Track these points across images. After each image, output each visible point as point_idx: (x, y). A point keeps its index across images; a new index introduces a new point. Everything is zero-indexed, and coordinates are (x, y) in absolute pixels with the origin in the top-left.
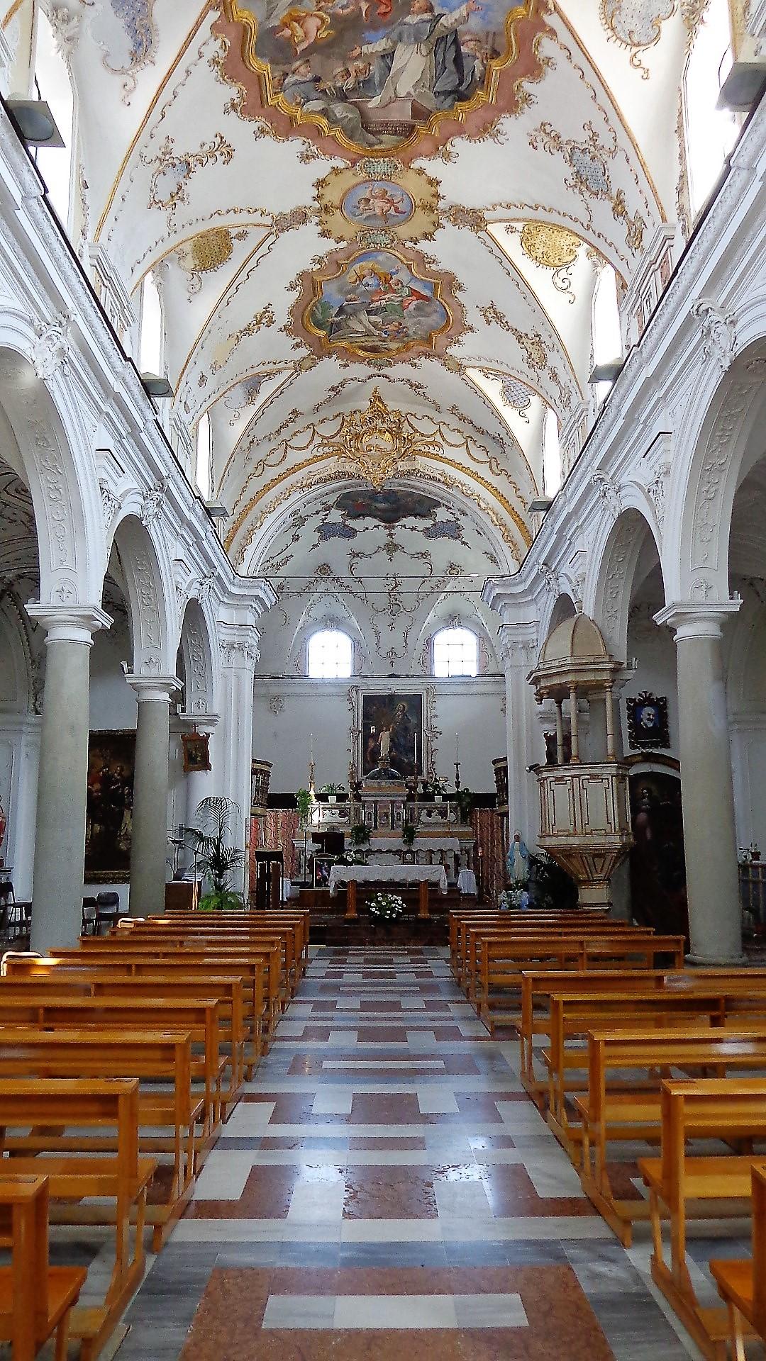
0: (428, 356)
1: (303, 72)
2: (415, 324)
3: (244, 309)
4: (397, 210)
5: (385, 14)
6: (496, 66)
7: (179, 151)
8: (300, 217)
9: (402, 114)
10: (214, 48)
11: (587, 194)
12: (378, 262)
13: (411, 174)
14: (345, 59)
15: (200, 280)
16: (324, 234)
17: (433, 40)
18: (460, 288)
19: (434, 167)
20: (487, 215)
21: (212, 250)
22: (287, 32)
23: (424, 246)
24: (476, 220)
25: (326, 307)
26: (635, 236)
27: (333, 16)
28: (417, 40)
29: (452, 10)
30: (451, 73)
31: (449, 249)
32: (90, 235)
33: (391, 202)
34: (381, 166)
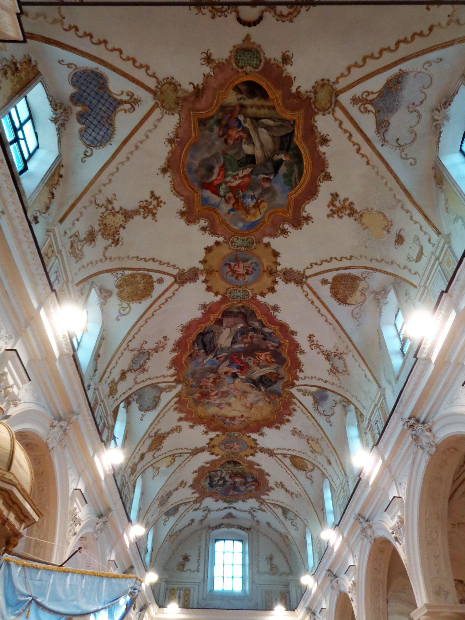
1: (270, 344)
2: (213, 144)
4: (230, 266)
9: (227, 321)
12: (243, 220)
14: (251, 343)
17: (216, 350)
18: (182, 214)
19: (211, 298)
20: (176, 286)
27: (255, 358)
33: (233, 271)
34: (239, 294)
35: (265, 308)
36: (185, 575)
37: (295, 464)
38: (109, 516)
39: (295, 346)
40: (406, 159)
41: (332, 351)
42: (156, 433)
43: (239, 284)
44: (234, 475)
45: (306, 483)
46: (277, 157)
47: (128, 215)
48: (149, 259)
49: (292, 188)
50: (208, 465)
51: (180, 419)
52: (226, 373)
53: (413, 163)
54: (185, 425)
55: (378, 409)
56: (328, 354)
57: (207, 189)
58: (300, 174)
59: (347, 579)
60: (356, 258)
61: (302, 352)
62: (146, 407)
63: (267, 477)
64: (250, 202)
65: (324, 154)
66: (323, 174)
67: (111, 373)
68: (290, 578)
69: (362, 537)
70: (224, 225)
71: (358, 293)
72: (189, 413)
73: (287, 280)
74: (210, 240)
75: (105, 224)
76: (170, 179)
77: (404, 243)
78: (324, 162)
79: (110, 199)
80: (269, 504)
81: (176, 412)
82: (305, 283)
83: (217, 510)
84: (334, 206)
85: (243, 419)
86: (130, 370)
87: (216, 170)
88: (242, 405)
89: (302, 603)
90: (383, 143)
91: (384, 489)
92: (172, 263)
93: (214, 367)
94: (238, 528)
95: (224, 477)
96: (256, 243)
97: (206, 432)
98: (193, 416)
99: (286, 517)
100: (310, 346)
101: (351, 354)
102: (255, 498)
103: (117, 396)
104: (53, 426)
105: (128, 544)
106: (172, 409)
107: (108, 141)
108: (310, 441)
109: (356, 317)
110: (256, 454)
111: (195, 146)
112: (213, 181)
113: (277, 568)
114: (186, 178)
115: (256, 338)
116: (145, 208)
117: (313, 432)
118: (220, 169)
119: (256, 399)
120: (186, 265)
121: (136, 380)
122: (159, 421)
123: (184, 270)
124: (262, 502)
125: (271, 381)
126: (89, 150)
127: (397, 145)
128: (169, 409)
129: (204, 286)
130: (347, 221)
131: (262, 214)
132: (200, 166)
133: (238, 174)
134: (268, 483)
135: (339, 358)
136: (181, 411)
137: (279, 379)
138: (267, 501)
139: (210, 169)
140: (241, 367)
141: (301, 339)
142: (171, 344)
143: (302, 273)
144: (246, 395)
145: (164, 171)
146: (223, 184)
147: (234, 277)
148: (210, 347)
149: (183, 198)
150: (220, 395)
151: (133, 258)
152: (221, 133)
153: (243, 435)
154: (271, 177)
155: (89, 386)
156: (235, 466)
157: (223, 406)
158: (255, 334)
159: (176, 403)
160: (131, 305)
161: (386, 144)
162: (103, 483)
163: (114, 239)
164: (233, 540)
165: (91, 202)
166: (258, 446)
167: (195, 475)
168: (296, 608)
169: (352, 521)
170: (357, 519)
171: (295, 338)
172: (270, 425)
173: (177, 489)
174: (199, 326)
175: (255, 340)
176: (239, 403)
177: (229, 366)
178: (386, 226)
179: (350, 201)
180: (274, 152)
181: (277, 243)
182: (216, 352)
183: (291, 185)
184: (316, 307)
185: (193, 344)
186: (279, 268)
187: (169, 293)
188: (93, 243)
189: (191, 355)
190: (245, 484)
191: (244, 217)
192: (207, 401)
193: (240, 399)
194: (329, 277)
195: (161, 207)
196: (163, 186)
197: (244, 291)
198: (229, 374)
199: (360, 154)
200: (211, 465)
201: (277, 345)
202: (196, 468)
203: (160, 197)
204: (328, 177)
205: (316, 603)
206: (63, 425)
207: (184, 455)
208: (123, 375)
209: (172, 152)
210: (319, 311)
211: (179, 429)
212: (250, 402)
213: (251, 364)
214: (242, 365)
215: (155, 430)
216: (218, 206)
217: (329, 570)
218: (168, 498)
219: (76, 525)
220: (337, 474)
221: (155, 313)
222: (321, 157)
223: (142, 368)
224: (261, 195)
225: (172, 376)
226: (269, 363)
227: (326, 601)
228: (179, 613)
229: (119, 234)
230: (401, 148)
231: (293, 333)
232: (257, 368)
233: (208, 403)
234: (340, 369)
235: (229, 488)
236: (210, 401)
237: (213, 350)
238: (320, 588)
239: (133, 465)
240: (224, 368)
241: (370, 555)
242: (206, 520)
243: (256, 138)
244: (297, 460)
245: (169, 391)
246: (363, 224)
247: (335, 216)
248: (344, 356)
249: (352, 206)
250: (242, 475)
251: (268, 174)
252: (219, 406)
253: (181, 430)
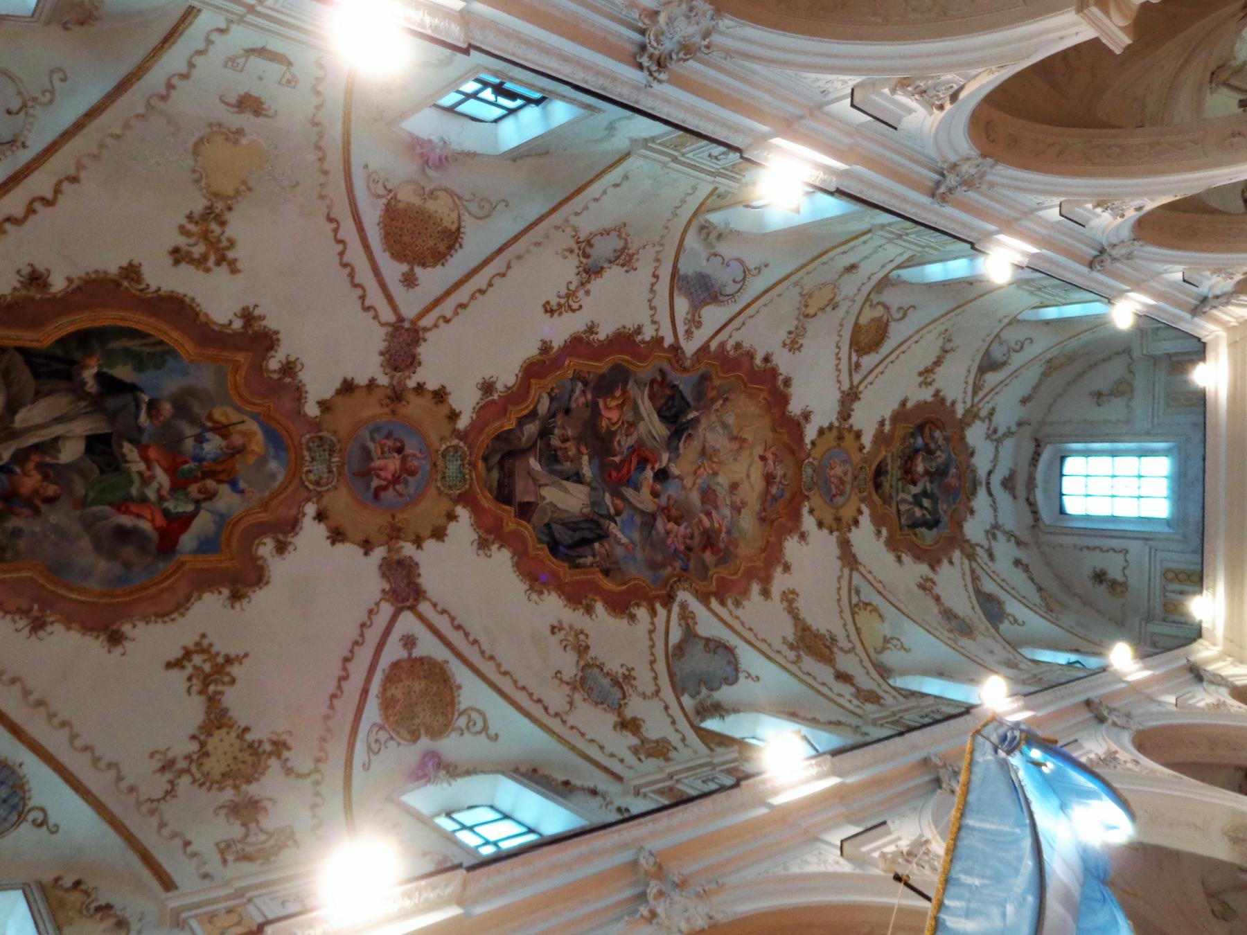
1: (579, 399)
2: (56, 529)
4: (379, 490)
5: (610, 476)
9: (523, 492)
12: (263, 460)
13: (445, 505)
14: (580, 439)
15: (379, 197)
17: (596, 517)
18: (236, 597)
19: (463, 528)
22: (618, 393)
27: (614, 434)
29: (622, 531)
34: (453, 468)
36: (1132, 581)
37: (875, 345)
38: (939, 763)
39: (577, 344)
40: (52, 92)
41: (577, 263)
42: (791, 647)
43: (428, 467)
44: (909, 476)
45: (915, 319)
46: (91, 386)
47: (217, 719)
48: (345, 669)
49: (172, 352)
50: (884, 531)
51: (766, 593)
52: (655, 494)
53: (61, 75)
54: (780, 582)
55: (683, 155)
56: (587, 271)
57: (175, 542)
58: (133, 333)
59: (1095, 222)
60: (329, 207)
61: (591, 329)
62: (729, 669)
63: (909, 405)
64: (213, 445)
65: (70, 280)
66: (126, 283)
67: (612, 755)
68: (1136, 354)
69: (984, 187)
70: (275, 502)
71: (431, 206)
72: (750, 574)
73: (412, 363)
74: (312, 533)
75: (223, 775)
76: (141, 625)
77: (255, 93)
78: (94, 280)
79: (160, 765)
80: (976, 400)
81: (745, 603)
82: (414, 322)
83: (995, 510)
84: (204, 258)
85: (769, 456)
86: (619, 709)
87: (126, 520)
88: (735, 459)
89: (1183, 326)
90: (19, 144)
91: (850, 135)
92: (364, 618)
93: (638, 520)
94: (1035, 466)
95: (915, 496)
96: (320, 431)
97: (803, 536)
98: (760, 564)
99: (1004, 364)
100: (574, 311)
101: (574, 220)
102: (963, 430)
103: (675, 739)
104: (654, 914)
105: (1028, 714)
106: (739, 612)
107: (13, 772)
108: (811, 311)
109: (488, 210)
110: (855, 428)
111: (58, 570)
112: (156, 529)
113: (1119, 382)
114: (143, 588)
115: (564, 429)
116: (206, 680)
117: (787, 305)
118: (124, 513)
120: (374, 585)
121: (649, 693)
122: (764, 641)
123: (383, 591)
124: (972, 414)
125: (672, 398)
126: (30, 817)
127: (22, 114)
128: (737, 618)
129: (430, 544)
130: (237, 226)
131: (245, 418)
132: (111, 555)
133: (140, 474)
134: (926, 402)
135: (591, 246)
136: (745, 592)
138: (968, 405)
139: (123, 534)
140: (638, 463)
141: (560, 330)
142: (573, 617)
143: (390, 329)
144: (709, 451)
145: (116, 639)
146: (166, 504)
147: (409, 478)
148: (590, 529)
149: (195, 595)
150: (708, 507)
151: (331, 707)
152: (26, 511)
153: (809, 455)
154: (146, 398)
155: (619, 810)
156: (886, 472)
157: (738, 500)
158: (556, 431)
159: (723, 603)
160: (462, 707)
161: (22, 139)
162: (850, 780)
163: (270, 754)
164: (1062, 475)
165: (152, 812)
166: (836, 424)
167: (906, 558)
168: (1199, 340)
169: (949, 210)
170: (943, 199)
171: (557, 343)
172: (784, 400)
173: (937, 599)
174: (532, 553)
175: (570, 432)
176: (730, 465)
177: (637, 488)
178: (227, 139)
179: (184, 221)
180: (78, 390)
181: (318, 385)
182: (602, 516)
183: (164, 353)
184: (473, 297)
185: (578, 566)
186: (383, 380)
187: (443, 624)
188: (264, 803)
189: (606, 573)
190: (930, 452)
191: (252, 459)
192: (723, 535)
194: (393, 270)
195: (211, 645)
196: (153, 640)
197: (444, 456)
198: (658, 487)
199: (55, 198)
200: (884, 524)
201: (580, 385)
202: (890, 557)
203: (185, 648)
204: (132, 272)
205: (1181, 296)
206: (655, 890)
207: (854, 582)
208: (629, 725)
209: (68, 622)
210: (482, 292)
211: (791, 596)
213: (631, 440)
214: (634, 460)
215: (785, 649)
216: (222, 516)
217: (1091, 265)
218: (956, 617)
219: (927, 853)
220: (875, 252)
221: (487, 654)
222: (79, 288)
223: (623, 682)
224: (194, 421)
225: (653, 613)
226: (627, 402)
227: (1166, 271)
228: (1214, 594)
229: (260, 742)
230: (30, 104)
231: (546, 348)
232: (642, 427)
233: (728, 533)
234: (619, 244)
235: (940, 485)
236: (724, 530)
237: (596, 523)
238: (1138, 286)
239: (857, 697)
240: (643, 499)
241: (1026, 167)
242: (1017, 534)
243: (42, 432)
244: (864, 339)
245: (693, 618)
246: (237, 191)
247: (231, 255)
248: (583, 236)
249: (196, 215)
250: (908, 459)
251: (138, 406)
252: (737, 509)
253: (793, 592)
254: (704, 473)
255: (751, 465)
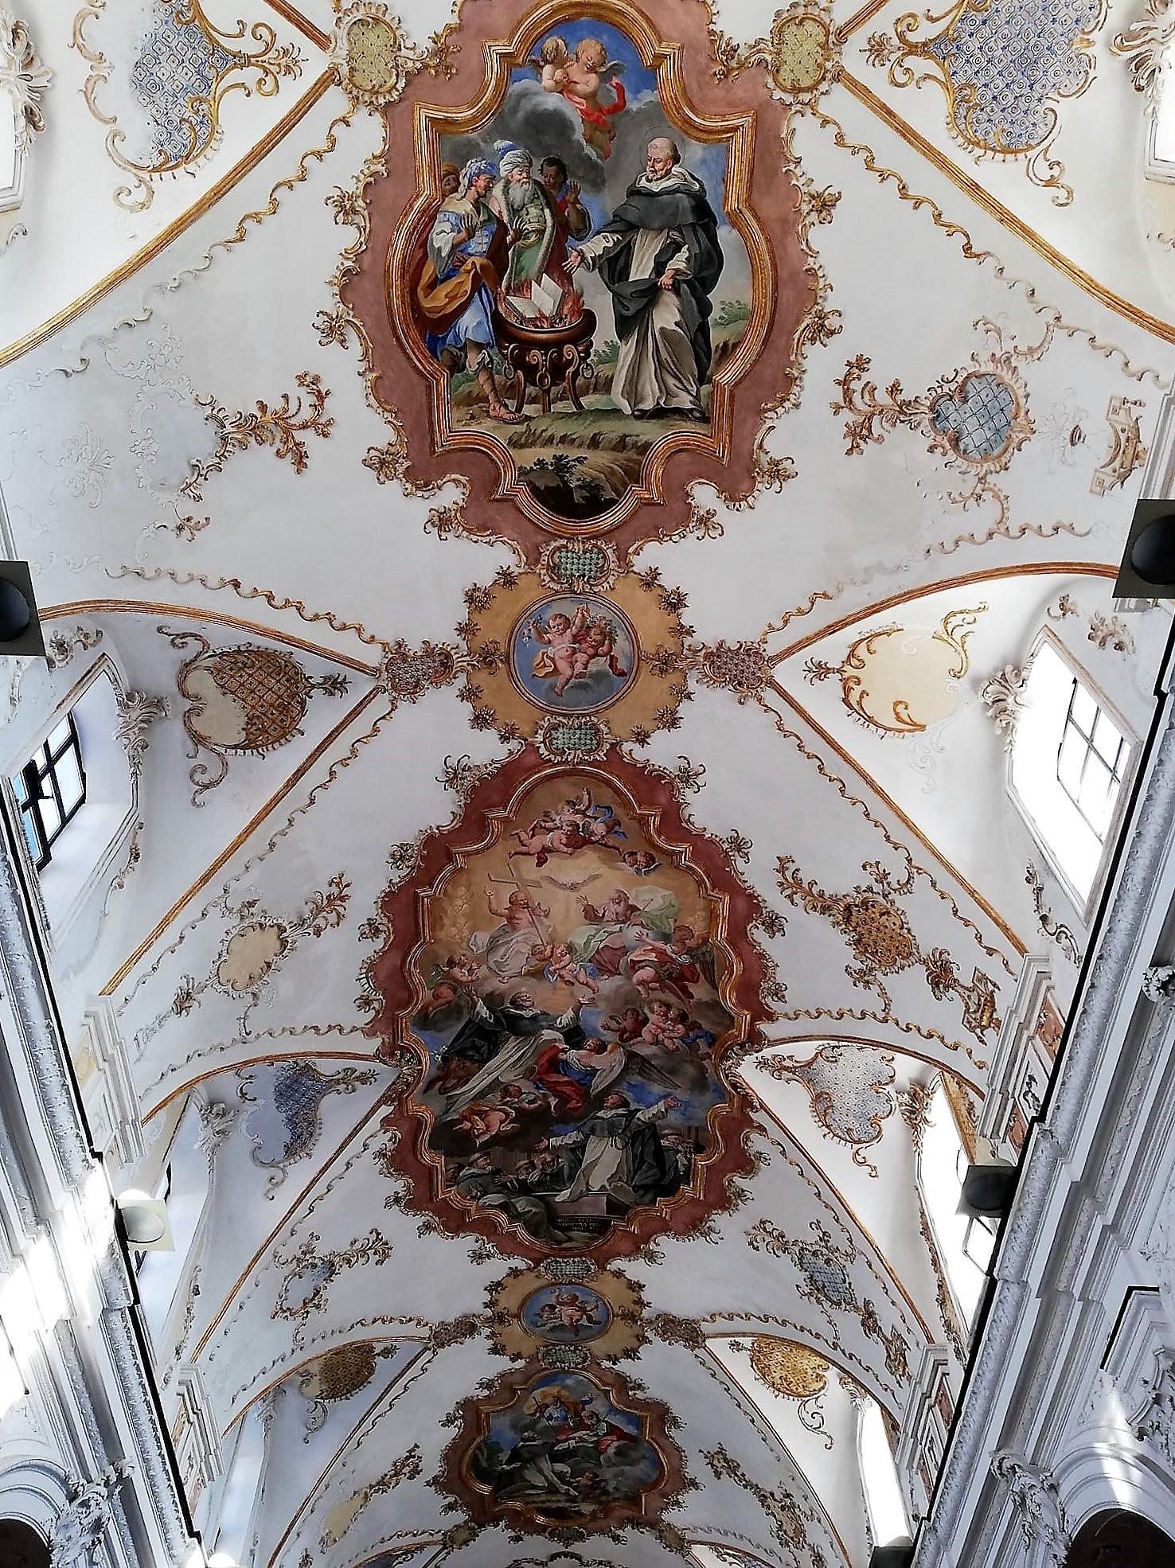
0: (636, 1523)
1: (481, 1164)
2: (616, 1476)
3: (380, 1452)
4: (589, 1318)
5: (575, 1109)
6: (701, 1162)
7: (322, 1250)
8: (466, 1327)
10: (383, 1140)
11: (827, 1304)
12: (565, 1387)
13: (608, 1277)
14: (531, 1151)
15: (325, 1411)
16: (495, 1350)
18: (675, 1423)
19: (634, 1269)
20: (705, 1327)
21: (347, 1372)
22: (467, 1125)
23: (625, 1366)
24: (689, 1333)
25: (494, 1449)
26: (897, 1359)
28: (611, 1134)
30: (650, 1167)
31: (657, 1368)
32: (186, 1354)
33: (583, 1310)
34: (570, 1267)
35: (508, 1246)
52: (601, 1048)
72: (738, 935)
93: (636, 1079)
119: (497, 956)
137: (438, 1079)
157: (614, 908)
166: (461, 681)
182: (627, 1126)
191: (564, 1392)
192: (668, 948)
193: (552, 941)
212: (518, 936)
213: (526, 1086)
214: (554, 1078)
233: (666, 938)
236: (660, 945)
240: (608, 1065)
254: (571, 967)
255: (553, 881)
